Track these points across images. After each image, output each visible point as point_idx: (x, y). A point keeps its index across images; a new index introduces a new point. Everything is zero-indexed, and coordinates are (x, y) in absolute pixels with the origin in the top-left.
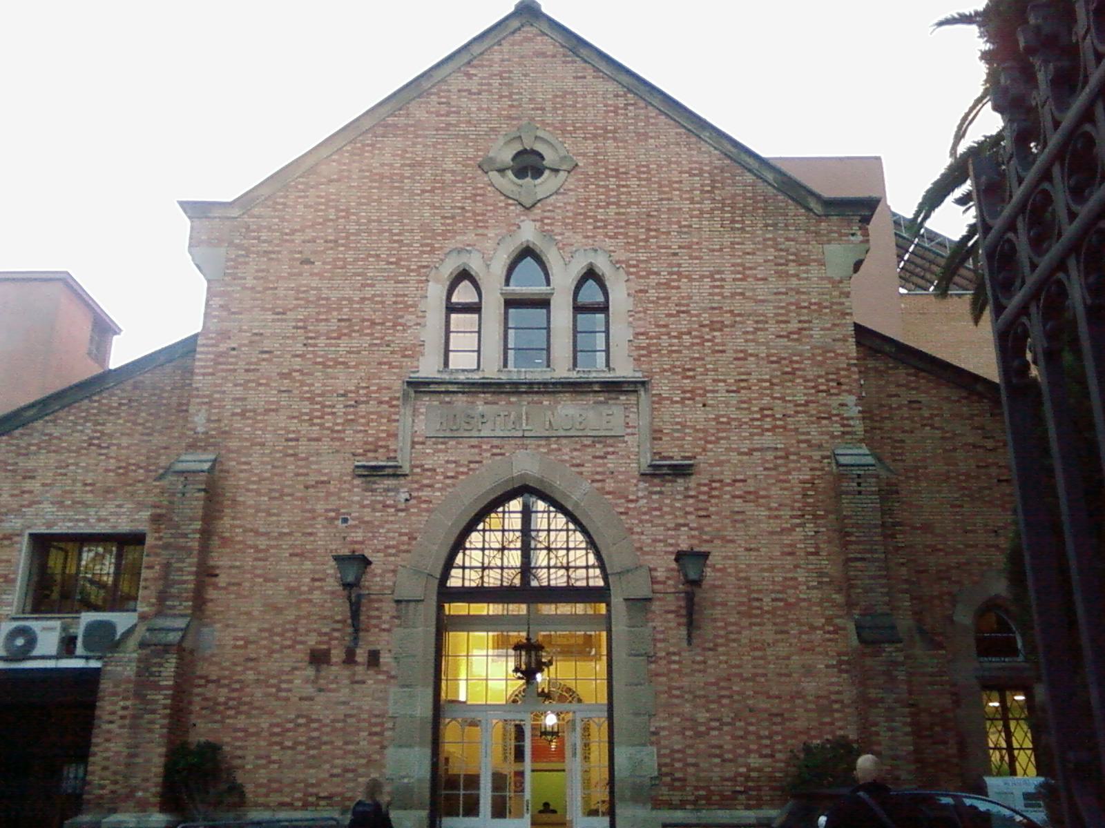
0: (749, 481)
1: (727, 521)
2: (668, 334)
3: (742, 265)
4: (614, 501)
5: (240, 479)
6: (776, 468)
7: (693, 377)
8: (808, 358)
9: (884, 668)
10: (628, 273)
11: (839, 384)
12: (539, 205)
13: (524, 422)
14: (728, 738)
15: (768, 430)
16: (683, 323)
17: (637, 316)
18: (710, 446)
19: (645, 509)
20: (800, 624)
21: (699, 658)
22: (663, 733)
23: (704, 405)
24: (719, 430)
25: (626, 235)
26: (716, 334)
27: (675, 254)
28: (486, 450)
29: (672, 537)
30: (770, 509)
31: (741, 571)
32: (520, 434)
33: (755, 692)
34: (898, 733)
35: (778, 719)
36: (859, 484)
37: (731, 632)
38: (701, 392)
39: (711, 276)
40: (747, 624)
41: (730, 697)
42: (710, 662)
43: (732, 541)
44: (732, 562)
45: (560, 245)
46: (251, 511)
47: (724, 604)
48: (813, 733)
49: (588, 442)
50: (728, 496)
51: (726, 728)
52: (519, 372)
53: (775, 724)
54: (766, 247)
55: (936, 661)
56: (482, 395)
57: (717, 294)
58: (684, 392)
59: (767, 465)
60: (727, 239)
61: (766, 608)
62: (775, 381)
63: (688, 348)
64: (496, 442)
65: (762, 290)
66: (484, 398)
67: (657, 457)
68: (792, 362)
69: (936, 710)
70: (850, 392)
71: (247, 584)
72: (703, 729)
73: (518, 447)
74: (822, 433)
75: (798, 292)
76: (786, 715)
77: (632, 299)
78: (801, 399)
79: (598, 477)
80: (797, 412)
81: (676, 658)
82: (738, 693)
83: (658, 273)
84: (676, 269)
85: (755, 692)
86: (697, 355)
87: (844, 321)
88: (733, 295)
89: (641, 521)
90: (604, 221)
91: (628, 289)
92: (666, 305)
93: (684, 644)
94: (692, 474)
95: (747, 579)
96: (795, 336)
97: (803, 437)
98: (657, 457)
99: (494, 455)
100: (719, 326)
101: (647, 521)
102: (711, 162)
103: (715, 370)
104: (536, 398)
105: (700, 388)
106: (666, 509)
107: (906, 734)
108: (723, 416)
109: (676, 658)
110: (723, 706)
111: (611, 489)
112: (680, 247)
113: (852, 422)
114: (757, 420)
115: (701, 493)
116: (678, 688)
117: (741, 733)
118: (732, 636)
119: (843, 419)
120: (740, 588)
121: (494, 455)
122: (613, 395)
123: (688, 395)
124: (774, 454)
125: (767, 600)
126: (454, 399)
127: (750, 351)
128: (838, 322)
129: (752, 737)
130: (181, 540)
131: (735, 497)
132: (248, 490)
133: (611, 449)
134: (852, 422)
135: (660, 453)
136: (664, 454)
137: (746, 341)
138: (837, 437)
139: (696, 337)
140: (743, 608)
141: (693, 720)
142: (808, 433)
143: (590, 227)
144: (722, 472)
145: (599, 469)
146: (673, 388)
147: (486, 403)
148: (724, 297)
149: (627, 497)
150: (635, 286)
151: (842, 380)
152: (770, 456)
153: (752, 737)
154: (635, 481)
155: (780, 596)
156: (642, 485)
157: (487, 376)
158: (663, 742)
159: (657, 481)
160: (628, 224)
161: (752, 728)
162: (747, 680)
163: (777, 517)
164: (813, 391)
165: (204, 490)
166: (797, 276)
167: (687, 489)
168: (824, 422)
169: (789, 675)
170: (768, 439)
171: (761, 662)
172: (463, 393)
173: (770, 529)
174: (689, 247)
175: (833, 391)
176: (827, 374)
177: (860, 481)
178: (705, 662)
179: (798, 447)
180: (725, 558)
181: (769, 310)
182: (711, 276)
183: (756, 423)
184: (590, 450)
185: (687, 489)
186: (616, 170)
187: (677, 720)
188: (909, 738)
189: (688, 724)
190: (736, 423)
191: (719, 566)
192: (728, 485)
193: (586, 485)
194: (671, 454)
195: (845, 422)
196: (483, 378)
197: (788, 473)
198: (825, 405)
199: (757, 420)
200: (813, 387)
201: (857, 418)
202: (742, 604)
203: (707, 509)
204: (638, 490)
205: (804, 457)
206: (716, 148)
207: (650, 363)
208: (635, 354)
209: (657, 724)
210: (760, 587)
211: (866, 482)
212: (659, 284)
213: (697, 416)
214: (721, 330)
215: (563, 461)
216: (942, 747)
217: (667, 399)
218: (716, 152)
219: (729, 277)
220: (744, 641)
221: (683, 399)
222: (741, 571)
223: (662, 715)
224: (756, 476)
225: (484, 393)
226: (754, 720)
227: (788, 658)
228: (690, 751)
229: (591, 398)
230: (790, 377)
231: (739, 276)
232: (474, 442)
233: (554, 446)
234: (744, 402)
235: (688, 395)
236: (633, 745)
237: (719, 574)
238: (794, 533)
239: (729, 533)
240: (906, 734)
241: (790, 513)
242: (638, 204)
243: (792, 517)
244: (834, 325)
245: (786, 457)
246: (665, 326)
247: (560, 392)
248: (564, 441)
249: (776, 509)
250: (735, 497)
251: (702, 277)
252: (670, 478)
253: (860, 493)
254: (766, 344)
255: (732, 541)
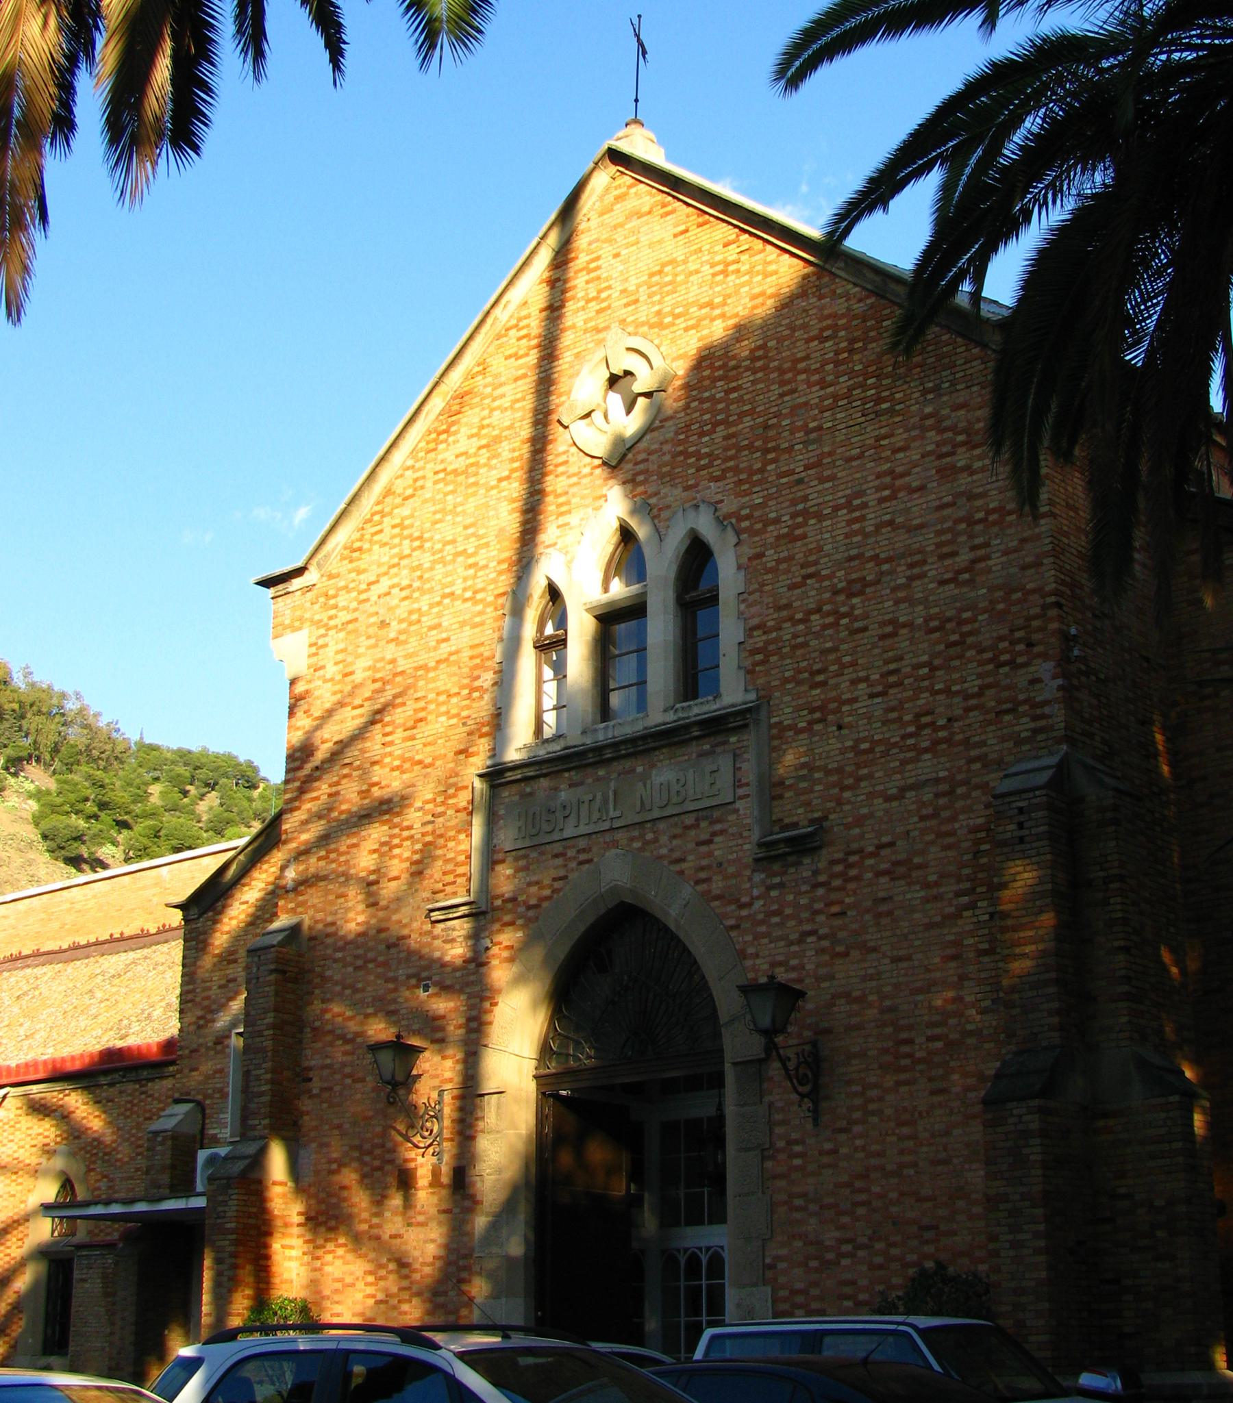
0: (899, 843)
1: (867, 917)
2: (790, 618)
3: (890, 472)
5: (327, 947)
6: (935, 815)
7: (823, 684)
10: (738, 533)
11: (1030, 645)
12: (630, 456)
13: (611, 806)
14: (864, 1268)
15: (926, 750)
16: (811, 595)
17: (751, 598)
18: (847, 794)
19: (761, 916)
21: (828, 1146)
22: (782, 1265)
23: (840, 728)
24: (858, 766)
25: (736, 470)
26: (855, 601)
28: (571, 859)
32: (606, 826)
35: (928, 1235)
36: (1021, 826)
39: (848, 505)
43: (874, 949)
44: (874, 983)
45: (655, 511)
46: (338, 988)
49: (689, 820)
51: (861, 1253)
52: (606, 728)
53: (927, 1242)
54: (924, 429)
55: (1163, 1115)
56: (566, 775)
57: (856, 533)
59: (924, 812)
60: (872, 431)
61: (918, 1055)
62: (937, 662)
63: (817, 635)
64: (582, 843)
66: (570, 779)
67: (776, 829)
68: (961, 623)
70: (1044, 656)
71: (337, 1088)
72: (830, 1256)
74: (1003, 739)
75: (971, 497)
76: (943, 1227)
78: (973, 685)
79: (703, 875)
80: (967, 710)
81: (798, 1148)
83: (777, 521)
84: (800, 507)
85: (902, 1194)
86: (829, 645)
87: (1037, 530)
88: (878, 528)
89: (757, 937)
90: (708, 455)
91: (738, 557)
92: (788, 571)
93: (809, 1126)
95: (892, 1009)
96: (966, 576)
97: (974, 753)
98: (776, 829)
99: (581, 863)
101: (764, 935)
102: (848, 309)
103: (853, 664)
104: (627, 764)
105: (834, 700)
106: (788, 911)
108: (864, 740)
109: (798, 1148)
111: (718, 892)
112: (807, 468)
113: (1047, 710)
114: (911, 735)
115: (834, 876)
116: (800, 1196)
117: (879, 1260)
118: (871, 1107)
119: (1035, 705)
121: (581, 863)
122: (720, 739)
123: (817, 715)
125: (920, 1040)
126: (536, 787)
127: (901, 619)
128: (1028, 534)
130: (258, 1040)
131: (879, 874)
132: (335, 961)
133: (718, 827)
134: (1047, 710)
135: (781, 820)
136: (787, 821)
137: (897, 603)
139: (828, 614)
140: (888, 1058)
143: (692, 471)
144: (862, 836)
145: (705, 862)
146: (798, 709)
147: (570, 786)
148: (866, 535)
149: (738, 900)
150: (747, 551)
151: (1036, 637)
152: (928, 796)
154: (748, 873)
155: (938, 1031)
156: (758, 877)
158: (782, 1280)
159: (776, 867)
161: (895, 1251)
163: (936, 898)
164: (991, 667)
165: (275, 971)
166: (968, 469)
167: (816, 873)
168: (1007, 718)
169: (946, 1162)
170: (927, 766)
172: (545, 775)
173: (926, 921)
174: (818, 464)
175: (1020, 660)
176: (1012, 631)
179: (969, 771)
180: (865, 978)
184: (693, 833)
185: (816, 873)
187: (798, 1244)
188: (1041, 1258)
190: (882, 748)
191: (856, 994)
192: (872, 855)
193: (687, 891)
194: (795, 819)
195: (1039, 711)
197: (953, 819)
198: (1008, 688)
199: (911, 735)
200: (990, 661)
202: (885, 1051)
203: (841, 902)
204: (752, 887)
205: (976, 787)
206: (855, 285)
211: (1031, 819)
212: (778, 538)
214: (861, 593)
215: (661, 857)
217: (790, 728)
218: (857, 289)
219: (871, 498)
224: (908, 832)
226: (898, 1238)
227: (947, 1133)
228: (815, 1292)
229: (693, 749)
230: (958, 649)
231: (886, 493)
232: (558, 848)
233: (649, 836)
234: (892, 709)
235: (817, 715)
237: (855, 1007)
238: (960, 922)
241: (955, 888)
242: (751, 412)
243: (958, 894)
244: (1023, 541)
245: (951, 793)
246: (788, 606)
247: (654, 749)
248: (662, 826)
249: (936, 884)
250: (879, 874)
251: (836, 509)
252: (791, 859)
253: (1022, 840)
255: (874, 949)
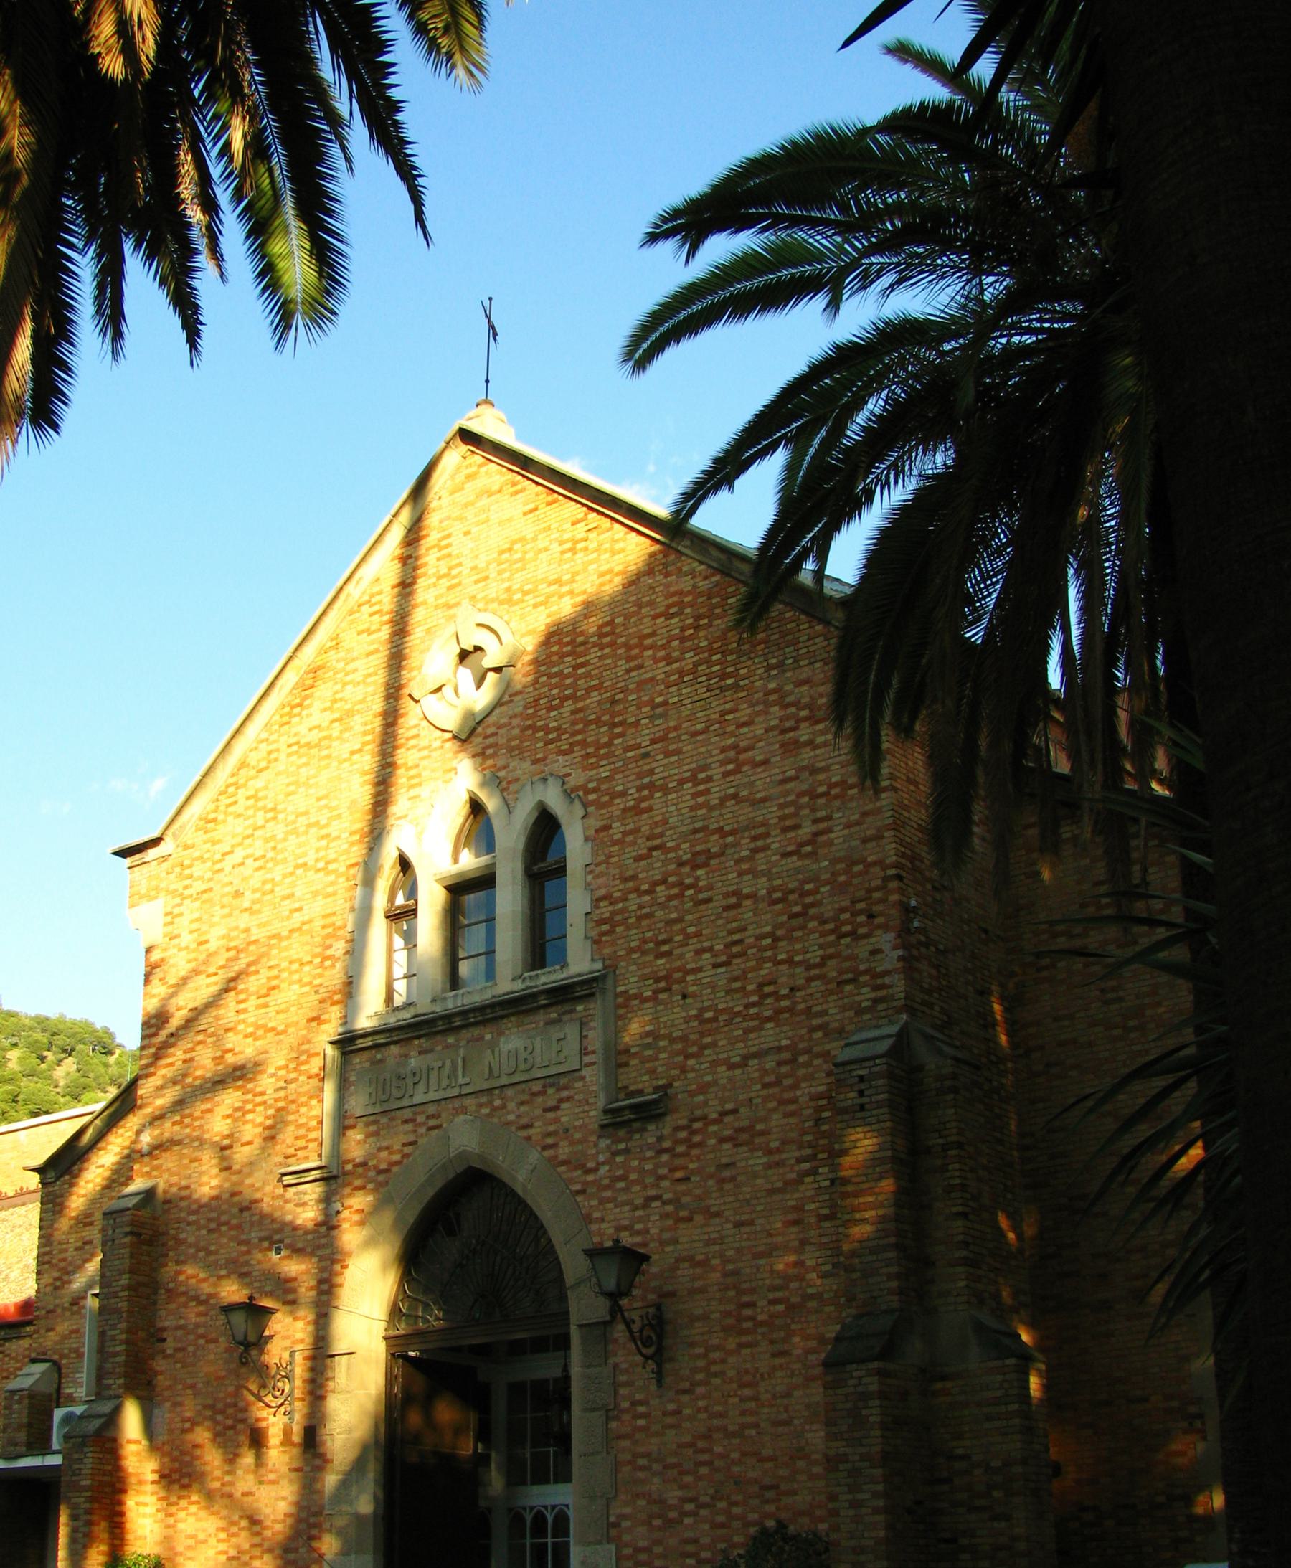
0: (742, 1110)
1: (711, 1182)
2: (637, 890)
3: (735, 747)
4: (570, 1175)
5: (181, 1210)
6: (778, 1083)
7: (668, 954)
8: (827, 883)
9: (849, 1405)
10: (585, 805)
11: (871, 916)
12: (480, 730)
13: (460, 1073)
14: (707, 1527)
15: (769, 1019)
16: (657, 867)
17: (598, 870)
18: (691, 1062)
19: (606, 1182)
20: (807, 1338)
21: (671, 1407)
22: (626, 1524)
23: (684, 997)
24: (702, 1034)
25: (584, 744)
26: (700, 872)
27: (646, 755)
28: (421, 1124)
29: (640, 1219)
30: (769, 1152)
31: (729, 1261)
32: (455, 1092)
33: (744, 1454)
34: (864, 1511)
35: (770, 1494)
36: (861, 1093)
37: (714, 1362)
38: (679, 975)
39: (693, 779)
40: (733, 1346)
41: (709, 1463)
42: (687, 1411)
43: (718, 1214)
44: (717, 1248)
45: (504, 784)
46: (192, 1251)
47: (705, 1317)
48: (818, 1513)
49: (536, 1087)
50: (713, 1141)
51: (703, 1512)
52: (455, 996)
53: (767, 1502)
54: (768, 705)
55: (999, 1378)
56: (416, 1042)
57: (700, 806)
58: (657, 980)
59: (767, 1079)
60: (717, 706)
61: (760, 1318)
62: (779, 933)
63: (663, 906)
64: (431, 1109)
65: (762, 781)
66: (420, 1046)
67: (622, 1096)
68: (803, 894)
69: (996, 1463)
70: (885, 927)
71: (191, 1349)
72: (673, 1515)
73: (457, 1112)
74: (844, 1009)
75: (814, 771)
76: (783, 1487)
77: (590, 844)
78: (815, 955)
79: (550, 1141)
80: (810, 980)
81: (641, 1409)
82: (722, 1456)
83: (623, 794)
84: (646, 780)
85: (744, 1454)
86: (674, 916)
87: (878, 804)
88: (723, 800)
89: (602, 1201)
90: (557, 729)
91: (585, 829)
92: (633, 843)
93: (653, 1387)
94: (664, 1114)
95: (736, 1273)
96: (809, 848)
97: (815, 1022)
98: (622, 1096)
99: (430, 1129)
100: (702, 858)
101: (609, 1200)
102: (694, 586)
103: (698, 934)
104: (476, 1032)
105: (678, 969)
106: (633, 1176)
107: (876, 1511)
108: (708, 1009)
109: (641, 1409)
110: (700, 1478)
111: (564, 1157)
112: (653, 742)
113: (887, 980)
114: (754, 1005)
115: (677, 1142)
116: (643, 1456)
117: (720, 1519)
118: (714, 1368)
119: (875, 976)
120: (727, 1288)
121: (430, 1129)
122: (567, 1007)
123: (662, 984)
124: (777, 1057)
125: (760, 1304)
126: (386, 1054)
127: (745, 891)
128: (870, 807)
129: (736, 1524)
130: (113, 1301)
131: (722, 1140)
132: (189, 1224)
133: (565, 1094)
134: (887, 980)
135: (626, 1087)
136: (632, 1088)
137: (740, 874)
138: (867, 1010)
139: (673, 885)
140: (730, 1321)
141: (662, 1502)
142: (825, 1013)
143: (540, 744)
144: (705, 1103)
145: (551, 1128)
146: (643, 978)
147: (420, 1053)
148: (711, 809)
149: (583, 1166)
150: (594, 823)
151: (876, 908)
152: (770, 1065)
153: (736, 1524)
154: (593, 1138)
155: (779, 1294)
156: (604, 1143)
157: (421, 1011)
158: (626, 1538)
159: (622, 1133)
160: (587, 724)
161: (736, 1510)
162: (734, 1434)
163: (778, 1164)
164: (832, 938)
165: (131, 1233)
166: (811, 743)
167: (660, 1139)
168: (848, 988)
169: (786, 1423)
170: (770, 1035)
171: (753, 1405)
172: (395, 1043)
173: (768, 1186)
174: (664, 739)
175: (862, 931)
176: (853, 902)
177: (863, 1086)
178: (678, 1412)
179: (811, 1039)
180: (708, 1243)
181: (771, 813)
182: (693, 779)
183: (753, 1011)
184: (540, 1099)
185: (660, 1139)
186: (572, 642)
187: (641, 1502)
188: (880, 1518)
189: (655, 1509)
190: (726, 1017)
191: (700, 1257)
192: (715, 1122)
193: (534, 1156)
194: (640, 1086)
195: (879, 981)
196: (416, 1016)
197: (795, 1087)
198: (849, 958)
199: (754, 1005)
200: (832, 932)
201: (896, 971)
202: (727, 1314)
203: (685, 1168)
204: (598, 1153)
205: (818, 1055)
206: (701, 563)
207: (613, 943)
208: (594, 933)
209: (618, 1511)
210: (754, 1284)
211: (871, 1087)
212: (625, 810)
213: (676, 1016)
214: (706, 865)
215: (509, 1123)
216: (1003, 1524)
217: (636, 996)
218: (702, 567)
219: (716, 772)
220: (731, 1373)
221: (656, 992)
222: (729, 1261)
223: (623, 1497)
224: (751, 1100)
225: (418, 1037)
226: (740, 1498)
227: (788, 1395)
228: (658, 1550)
229: (541, 1017)
230: (801, 920)
231: (731, 767)
232: (408, 1114)
233: (497, 1103)
234: (736, 979)
235: (662, 984)
236: (589, 1544)
237: (698, 1271)
238: (802, 1188)
239: (714, 1202)
240: (876, 1511)
241: (797, 1154)
242: (598, 688)
243: (799, 1160)
244: (865, 814)
245: (793, 1061)
246: (634, 877)
247: (502, 1017)
248: (509, 1092)
249: (778, 1150)
250: (722, 1140)
251: (682, 782)
252: (636, 1125)
253: (862, 1108)
254: (768, 874)
255: (718, 1214)
